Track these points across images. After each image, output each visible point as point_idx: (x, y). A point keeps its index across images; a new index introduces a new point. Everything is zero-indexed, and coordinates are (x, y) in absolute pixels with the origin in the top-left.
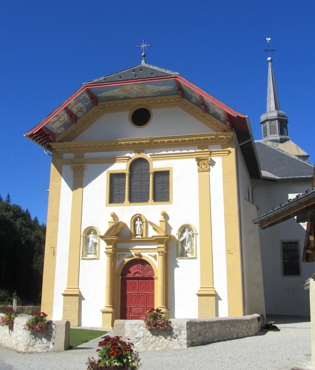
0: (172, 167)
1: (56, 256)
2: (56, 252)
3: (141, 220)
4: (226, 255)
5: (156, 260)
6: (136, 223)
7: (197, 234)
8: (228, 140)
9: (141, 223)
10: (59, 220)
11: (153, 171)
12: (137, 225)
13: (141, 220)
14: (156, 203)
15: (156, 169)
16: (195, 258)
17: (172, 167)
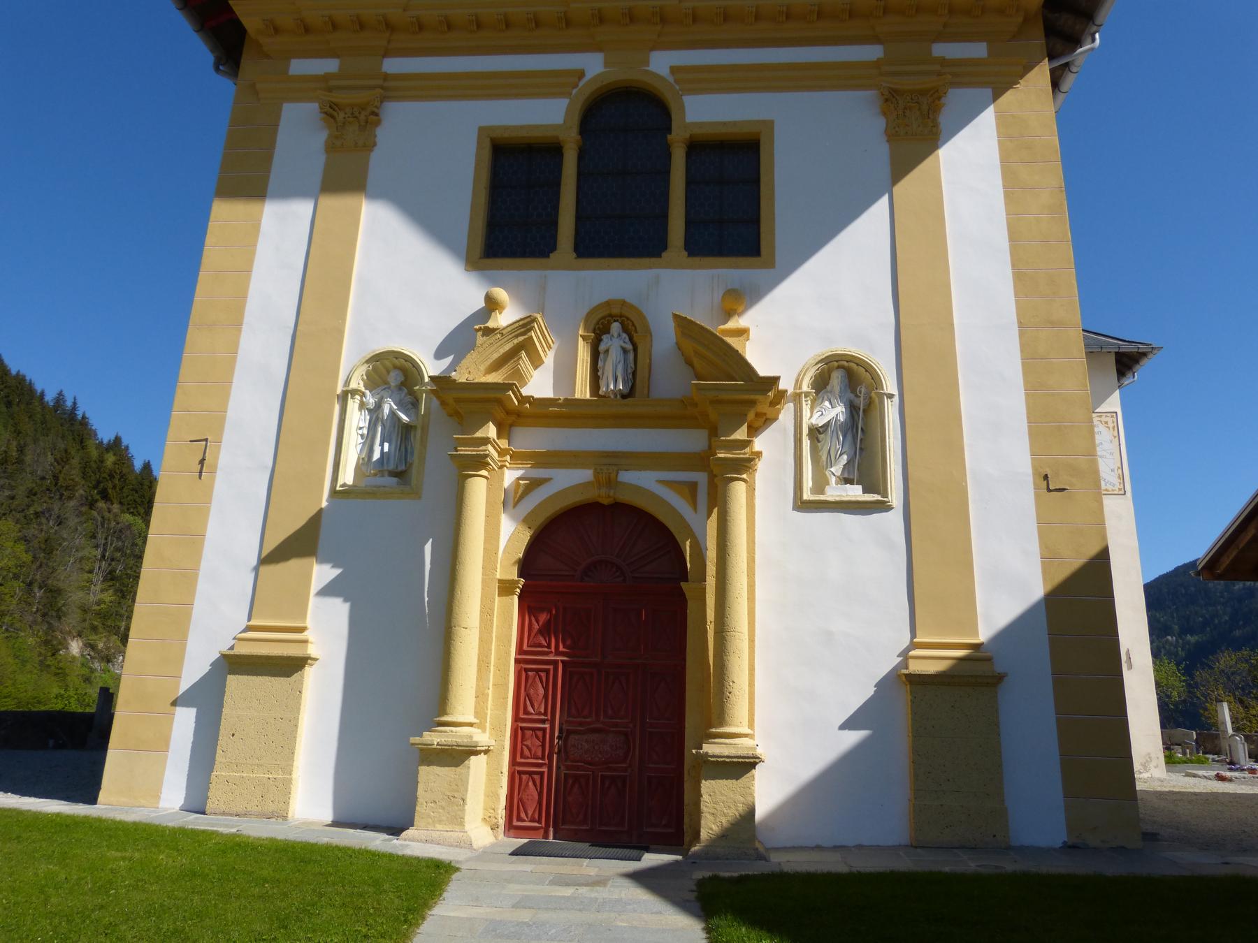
0: (772, 122)
1: (213, 479)
2: (217, 458)
3: (629, 329)
4: (1037, 496)
5: (695, 509)
6: (602, 347)
7: (890, 396)
8: (1020, 19)
9: (629, 346)
10: (246, 320)
11: (687, 136)
12: (607, 351)
13: (629, 329)
14: (697, 260)
15: (701, 125)
16: (883, 507)
17: (772, 122)
